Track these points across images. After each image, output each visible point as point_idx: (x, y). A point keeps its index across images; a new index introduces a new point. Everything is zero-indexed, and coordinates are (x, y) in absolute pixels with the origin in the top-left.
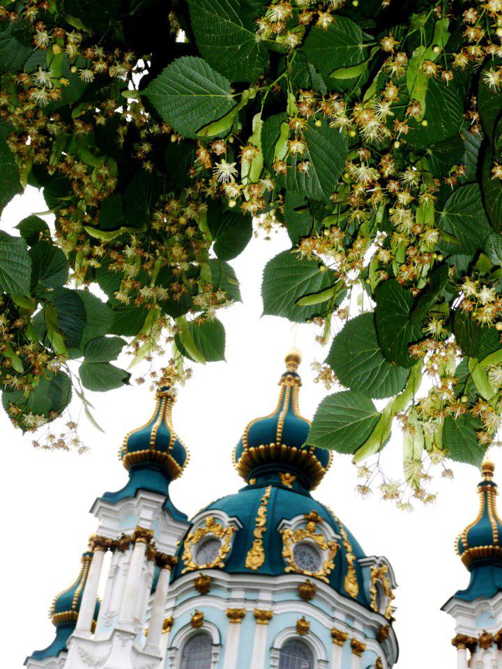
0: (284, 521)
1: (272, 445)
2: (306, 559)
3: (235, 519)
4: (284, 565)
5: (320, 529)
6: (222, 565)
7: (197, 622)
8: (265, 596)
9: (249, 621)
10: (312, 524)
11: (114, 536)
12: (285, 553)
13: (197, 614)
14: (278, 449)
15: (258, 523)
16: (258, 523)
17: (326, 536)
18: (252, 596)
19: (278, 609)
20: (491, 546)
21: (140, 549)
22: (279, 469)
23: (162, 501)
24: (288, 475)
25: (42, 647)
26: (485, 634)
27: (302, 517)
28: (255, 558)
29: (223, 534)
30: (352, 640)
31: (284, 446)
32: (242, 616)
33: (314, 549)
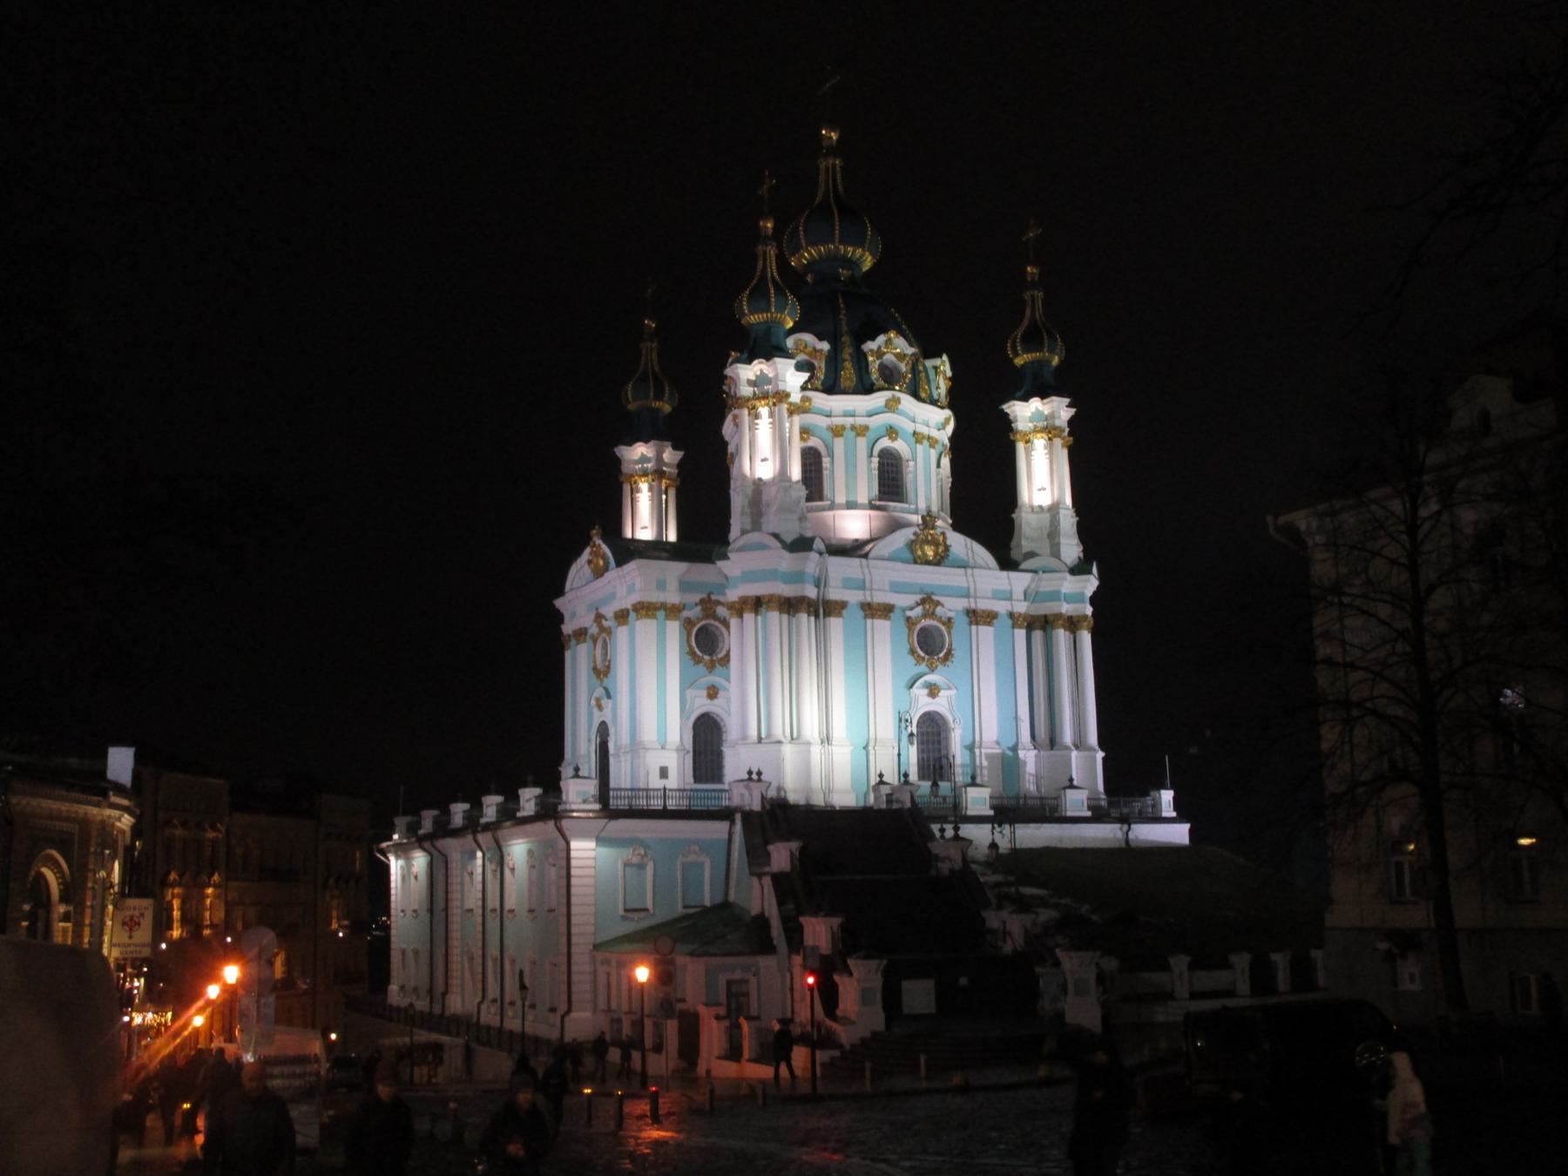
9: (850, 434)
19: (874, 422)
30: (929, 438)
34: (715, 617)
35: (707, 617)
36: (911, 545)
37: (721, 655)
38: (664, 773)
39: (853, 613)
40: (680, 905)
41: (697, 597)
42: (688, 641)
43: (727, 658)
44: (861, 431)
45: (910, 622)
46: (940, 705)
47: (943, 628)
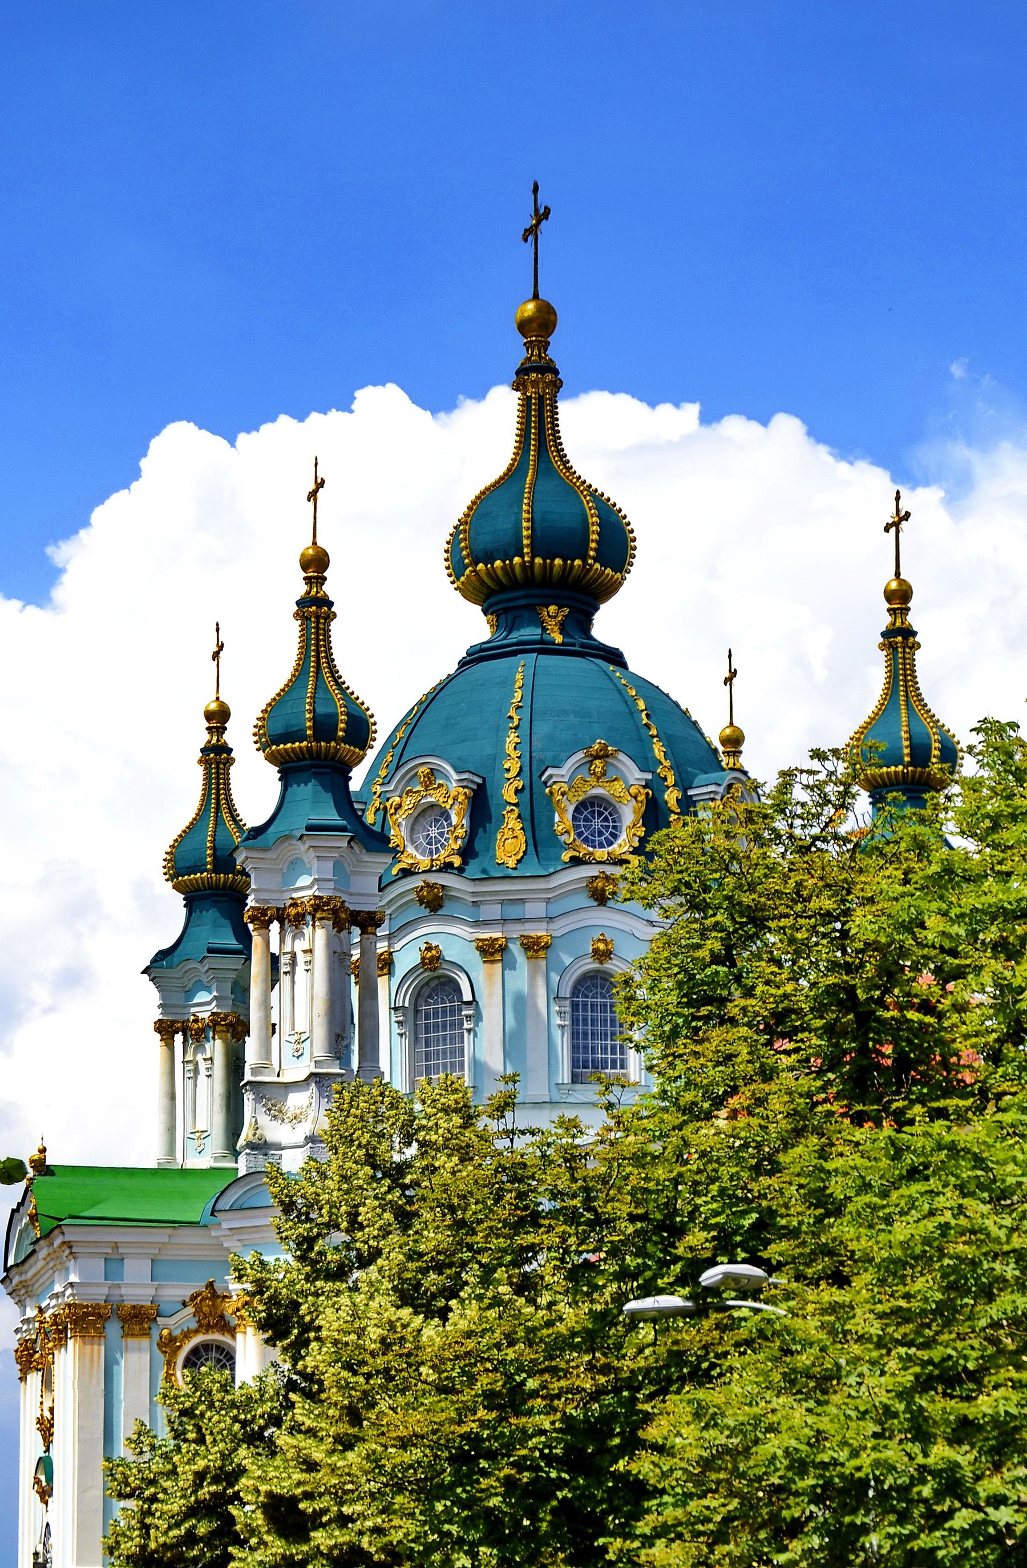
1: (517, 560)
3: (466, 776)
5: (616, 767)
6: (457, 861)
10: (597, 762)
13: (429, 949)
14: (528, 568)
15: (508, 770)
16: (508, 770)
17: (626, 781)
18: (513, 912)
20: (900, 768)
22: (538, 601)
24: (552, 609)
27: (580, 755)
28: (509, 843)
29: (450, 802)
31: (538, 560)
35: (208, 1328)
41: (187, 1293)
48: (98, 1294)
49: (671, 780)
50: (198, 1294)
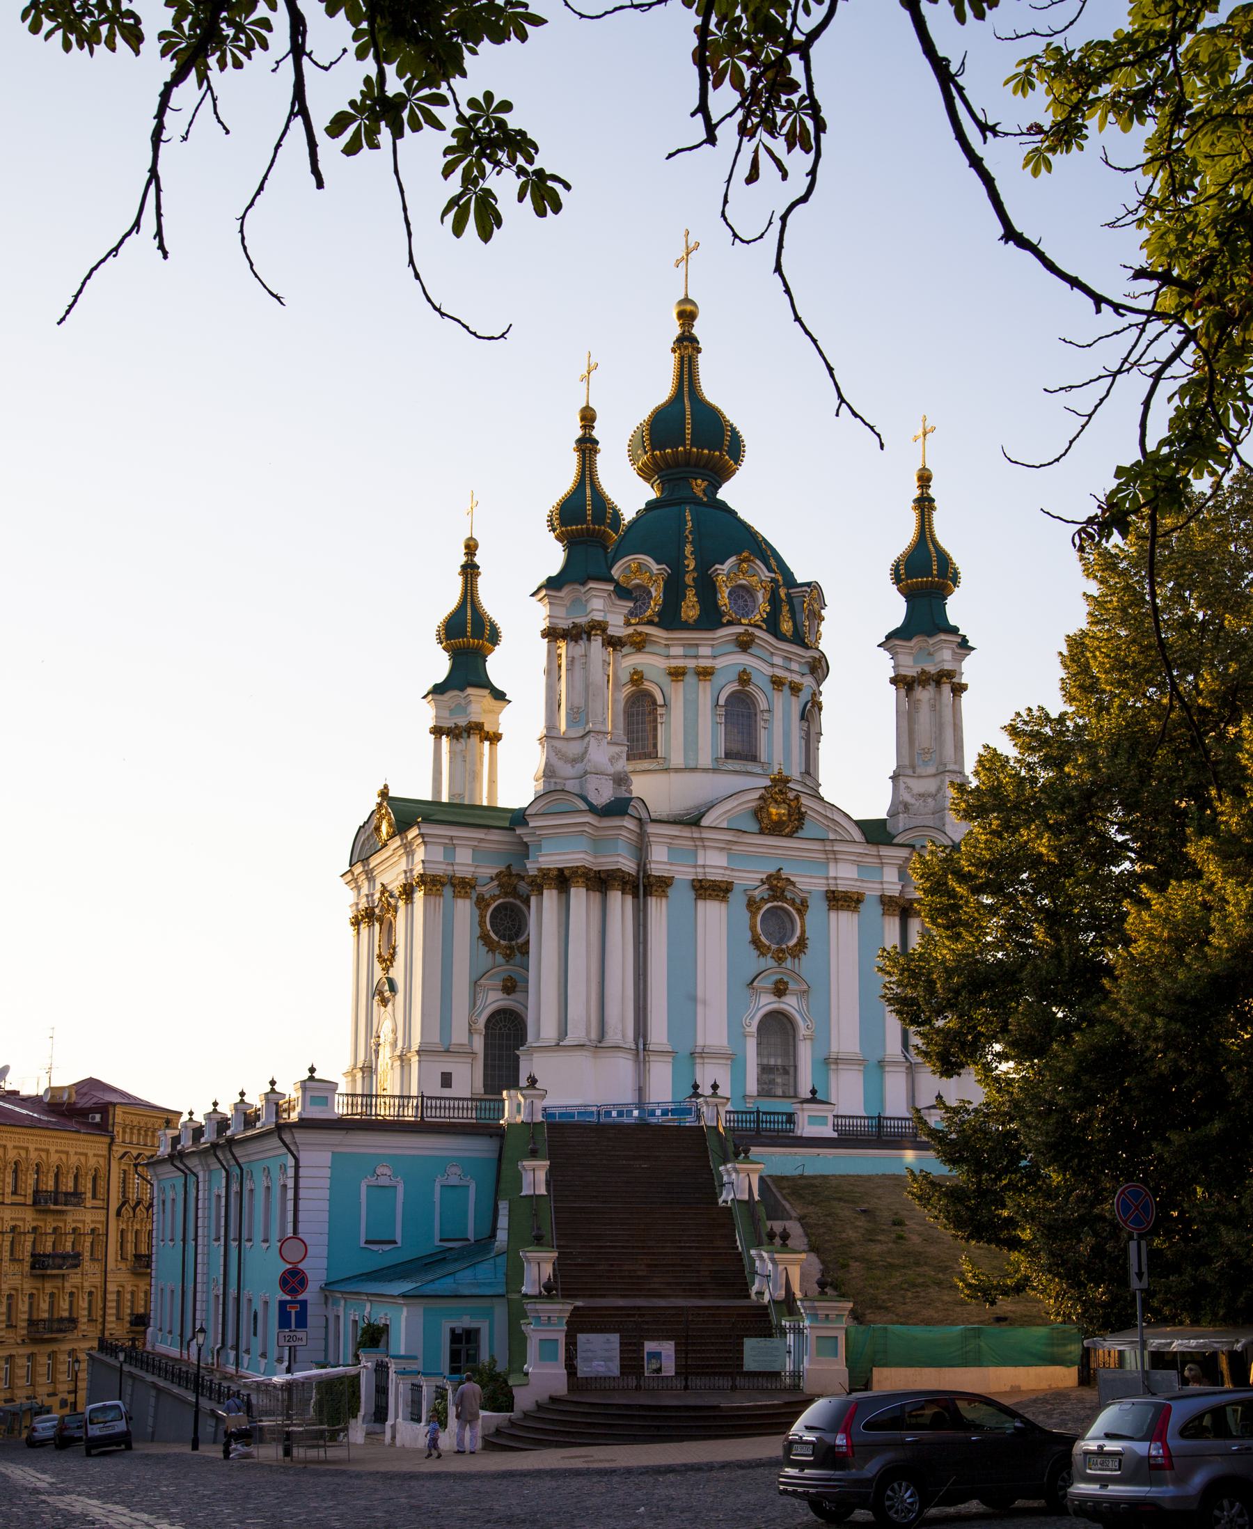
0: (717, 566)
2: (740, 602)
4: (722, 615)
6: (656, 619)
7: (637, 678)
8: (705, 651)
9: (690, 679)
11: (564, 624)
12: (721, 603)
13: (636, 672)
18: (692, 652)
19: (719, 663)
21: (597, 643)
23: (612, 588)
24: (699, 481)
25: (440, 679)
26: (923, 672)
27: (732, 560)
28: (690, 609)
32: (684, 674)
33: (748, 591)
34: (519, 897)
35: (506, 894)
36: (758, 813)
37: (521, 940)
38: (446, 1080)
39: (681, 894)
40: (437, 1238)
41: (496, 871)
42: (482, 923)
43: (528, 941)
44: (705, 673)
45: (752, 905)
46: (790, 1004)
47: (794, 912)
48: (440, 870)
49: (781, 582)
50: (501, 872)
